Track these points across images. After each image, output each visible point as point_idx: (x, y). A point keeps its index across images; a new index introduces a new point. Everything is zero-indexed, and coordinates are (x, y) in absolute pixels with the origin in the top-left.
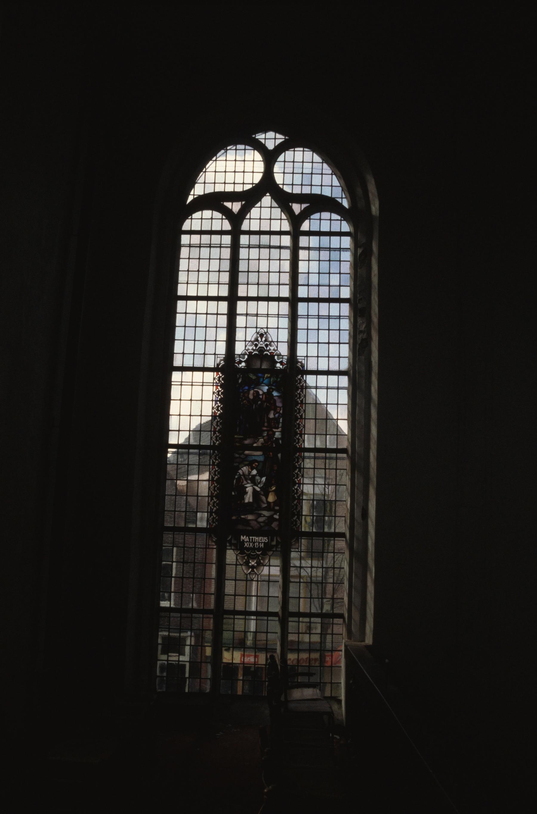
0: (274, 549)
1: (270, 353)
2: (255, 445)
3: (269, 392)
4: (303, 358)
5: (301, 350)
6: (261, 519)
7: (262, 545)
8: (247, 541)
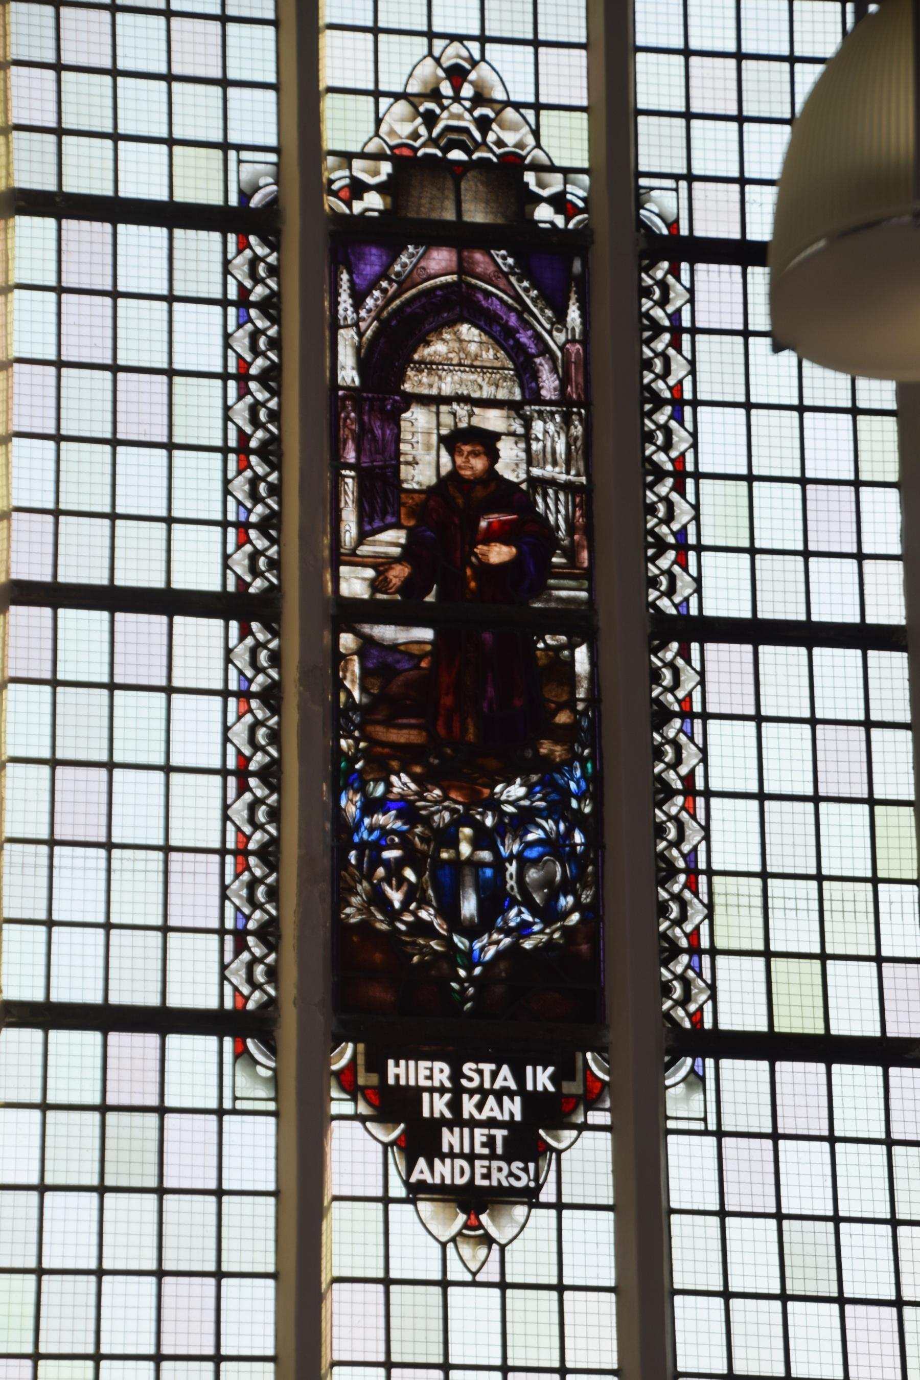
5: (657, 146)
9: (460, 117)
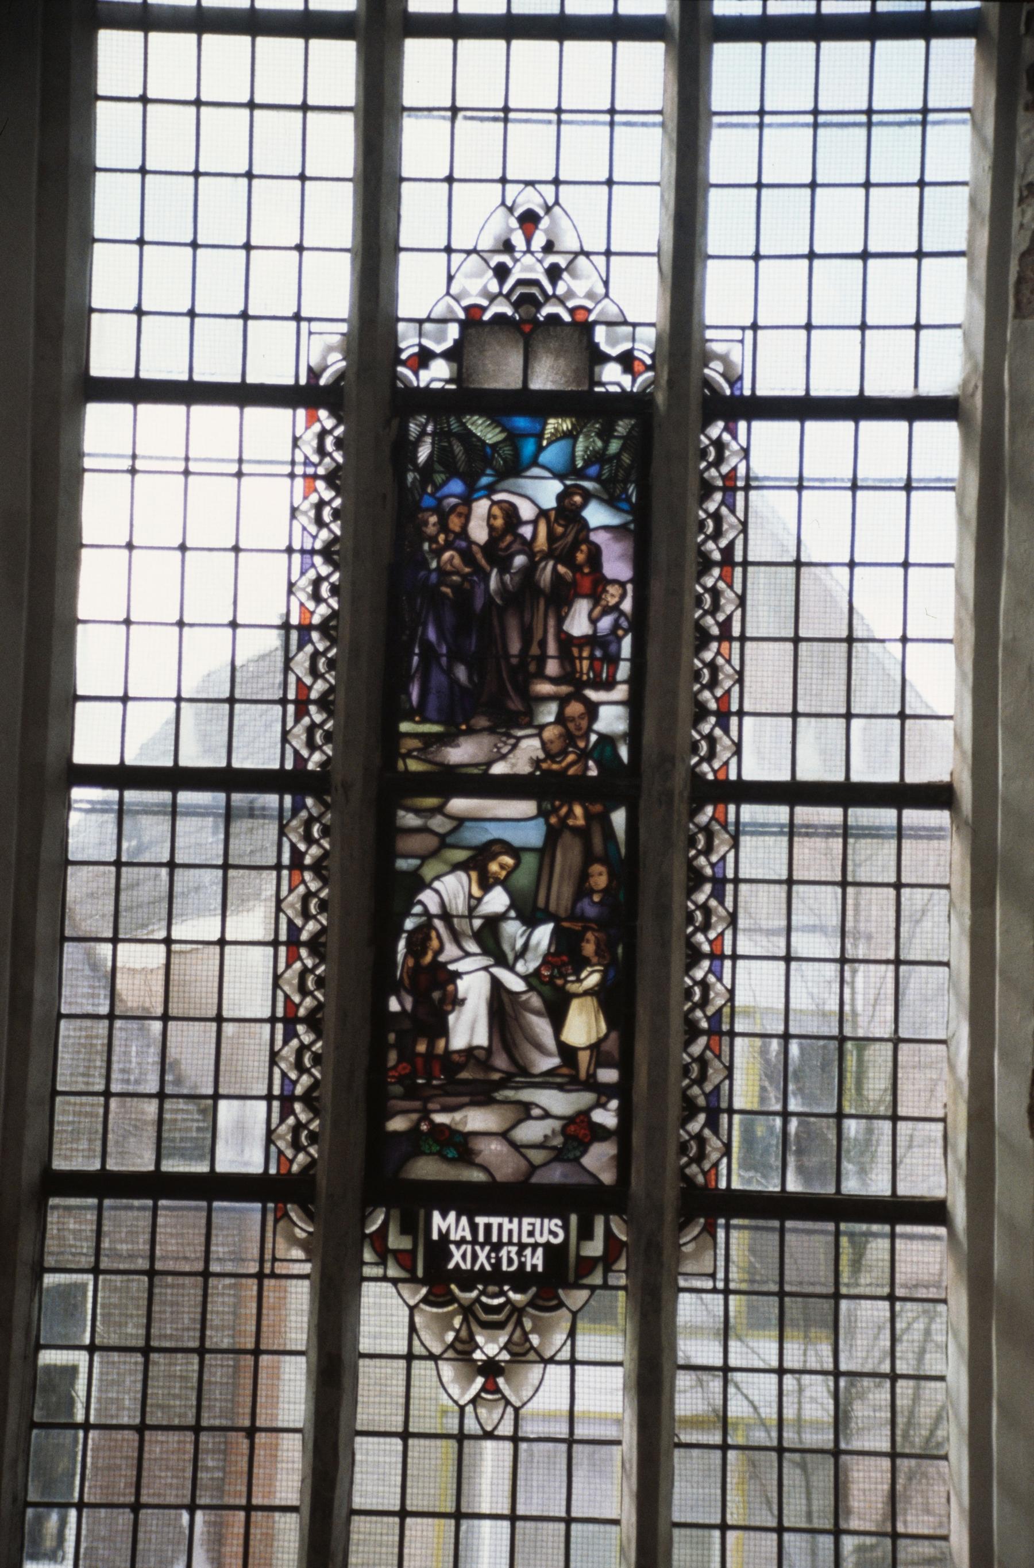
0: (597, 1279)
1: (572, 311)
2: (499, 769)
3: (567, 513)
4: (737, 334)
6: (531, 1132)
7: (536, 1260)
8: (463, 1241)
9: (531, 269)
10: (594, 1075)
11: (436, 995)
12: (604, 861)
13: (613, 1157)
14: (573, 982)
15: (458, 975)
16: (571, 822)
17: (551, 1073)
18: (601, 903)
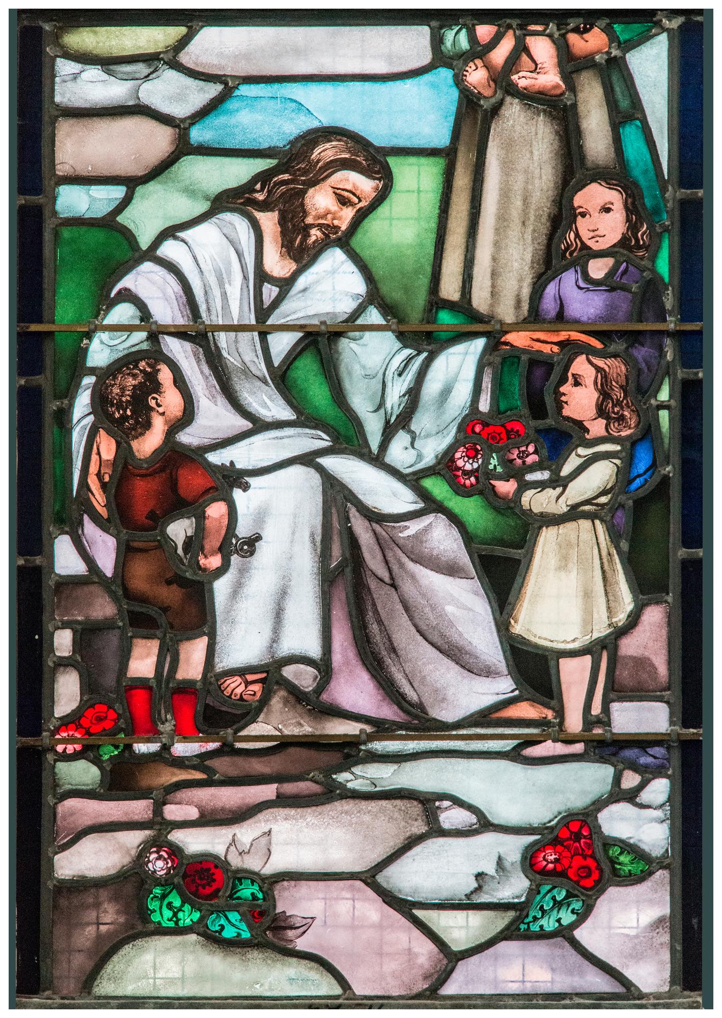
6: (436, 869)
10: (605, 720)
11: (179, 530)
12: (617, 174)
13: (660, 921)
14: (541, 485)
15: (235, 478)
16: (522, 80)
17: (485, 718)
18: (609, 284)
